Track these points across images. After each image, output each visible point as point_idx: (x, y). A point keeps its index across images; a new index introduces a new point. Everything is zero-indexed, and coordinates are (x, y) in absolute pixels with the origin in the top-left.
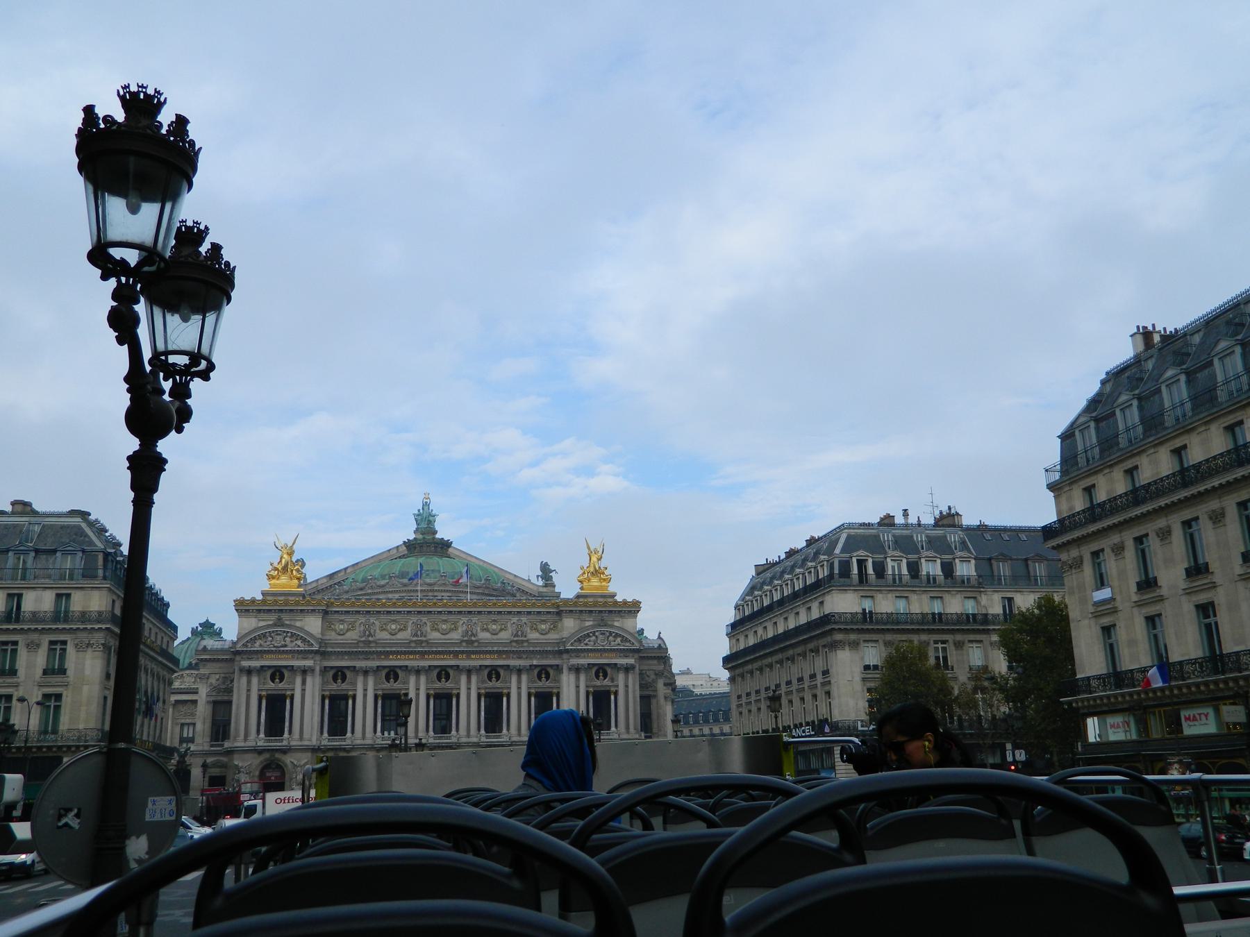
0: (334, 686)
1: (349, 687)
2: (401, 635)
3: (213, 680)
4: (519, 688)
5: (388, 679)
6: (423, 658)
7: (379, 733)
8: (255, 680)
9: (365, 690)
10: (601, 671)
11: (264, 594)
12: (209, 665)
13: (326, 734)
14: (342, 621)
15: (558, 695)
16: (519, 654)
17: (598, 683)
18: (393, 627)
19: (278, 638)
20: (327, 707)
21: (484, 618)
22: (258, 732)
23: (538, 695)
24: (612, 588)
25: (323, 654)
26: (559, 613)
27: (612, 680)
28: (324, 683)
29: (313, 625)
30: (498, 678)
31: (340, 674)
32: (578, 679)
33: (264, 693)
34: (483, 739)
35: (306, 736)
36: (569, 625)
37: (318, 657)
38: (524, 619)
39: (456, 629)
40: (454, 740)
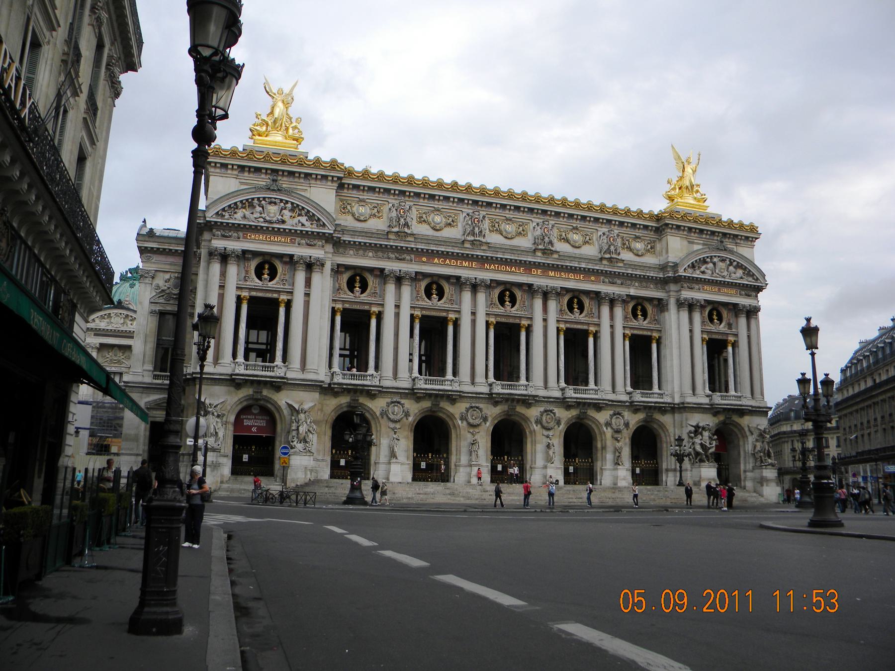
0: (349, 296)
1: (372, 299)
3: (161, 281)
8: (233, 270)
9: (397, 307)
10: (715, 311)
12: (155, 258)
16: (612, 277)
19: (273, 209)
22: (234, 356)
25: (338, 244)
31: (357, 279)
33: (245, 294)
35: (308, 366)
37: (329, 248)
38: (616, 230)
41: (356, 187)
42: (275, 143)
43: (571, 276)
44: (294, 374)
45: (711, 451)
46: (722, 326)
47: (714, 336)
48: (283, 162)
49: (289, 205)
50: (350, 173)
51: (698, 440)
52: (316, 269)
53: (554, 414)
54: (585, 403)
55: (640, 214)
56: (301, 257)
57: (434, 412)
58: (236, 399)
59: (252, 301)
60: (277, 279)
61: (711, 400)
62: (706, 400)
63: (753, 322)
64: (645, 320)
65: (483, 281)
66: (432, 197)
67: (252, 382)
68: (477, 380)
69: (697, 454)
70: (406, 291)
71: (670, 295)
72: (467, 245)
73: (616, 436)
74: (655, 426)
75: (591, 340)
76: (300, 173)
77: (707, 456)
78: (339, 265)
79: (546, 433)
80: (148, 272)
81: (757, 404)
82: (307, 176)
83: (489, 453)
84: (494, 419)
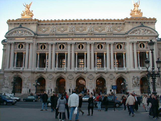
0: (41, 50)
4: (110, 51)
7: (57, 67)
11: (18, 19)
13: (38, 68)
14: (44, 28)
15: (125, 54)
17: (141, 49)
18: (62, 29)
20: (38, 58)
24: (143, 16)
25: (37, 38)
26: (124, 24)
28: (37, 49)
29: (34, 28)
31: (43, 46)
32: (133, 48)
33: (16, 52)
34: (96, 70)
36: (128, 27)
37: (35, 39)
38: (111, 26)
40: (85, 70)
41: (42, 24)
43: (98, 39)
44: (26, 69)
45: (138, 84)
46: (144, 48)
47: (141, 51)
48: (24, 21)
49: (24, 31)
50: (41, 21)
52: (30, 45)
53: (93, 76)
54: (101, 72)
55: (118, 20)
56: (28, 42)
57: (60, 76)
58: (12, 76)
59: (18, 53)
60: (23, 48)
61: (139, 69)
64: (121, 49)
66: (60, 24)
67: (16, 72)
68: (72, 68)
69: (134, 85)
71: (128, 41)
74: (124, 77)
76: (28, 23)
77: (136, 85)
78: (38, 43)
79: (90, 80)
80: (4, 49)
82: (29, 23)
84: (76, 77)
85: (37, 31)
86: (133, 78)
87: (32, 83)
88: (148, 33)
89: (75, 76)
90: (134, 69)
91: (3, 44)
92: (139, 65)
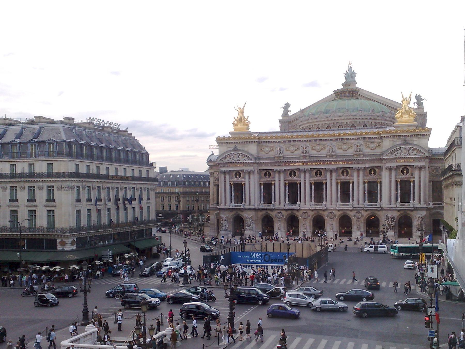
1: (272, 179)
2: (296, 153)
5: (291, 175)
6: (307, 164)
8: (227, 177)
10: (405, 169)
12: (214, 167)
13: (262, 202)
16: (358, 162)
17: (403, 176)
18: (292, 148)
19: (236, 156)
20: (262, 189)
21: (340, 142)
23: (369, 182)
25: (259, 163)
27: (412, 175)
28: (260, 178)
30: (347, 174)
31: (268, 173)
33: (232, 183)
36: (387, 144)
37: (255, 165)
38: (361, 142)
39: (324, 148)
42: (240, 129)
43: (341, 163)
44: (247, 206)
47: (404, 179)
48: (239, 139)
51: (386, 222)
62: (395, 206)
63: (423, 172)
65: (308, 169)
70: (282, 176)
72: (301, 158)
73: (358, 220)
75: (351, 185)
81: (421, 206)
83: (312, 227)
84: (313, 216)
85: (258, 153)
86: (386, 217)
87: (256, 224)
88: (413, 154)
89: (311, 213)
90: (389, 206)
91: (209, 165)
92: (399, 199)
